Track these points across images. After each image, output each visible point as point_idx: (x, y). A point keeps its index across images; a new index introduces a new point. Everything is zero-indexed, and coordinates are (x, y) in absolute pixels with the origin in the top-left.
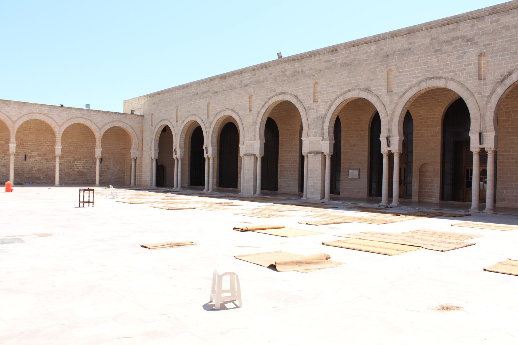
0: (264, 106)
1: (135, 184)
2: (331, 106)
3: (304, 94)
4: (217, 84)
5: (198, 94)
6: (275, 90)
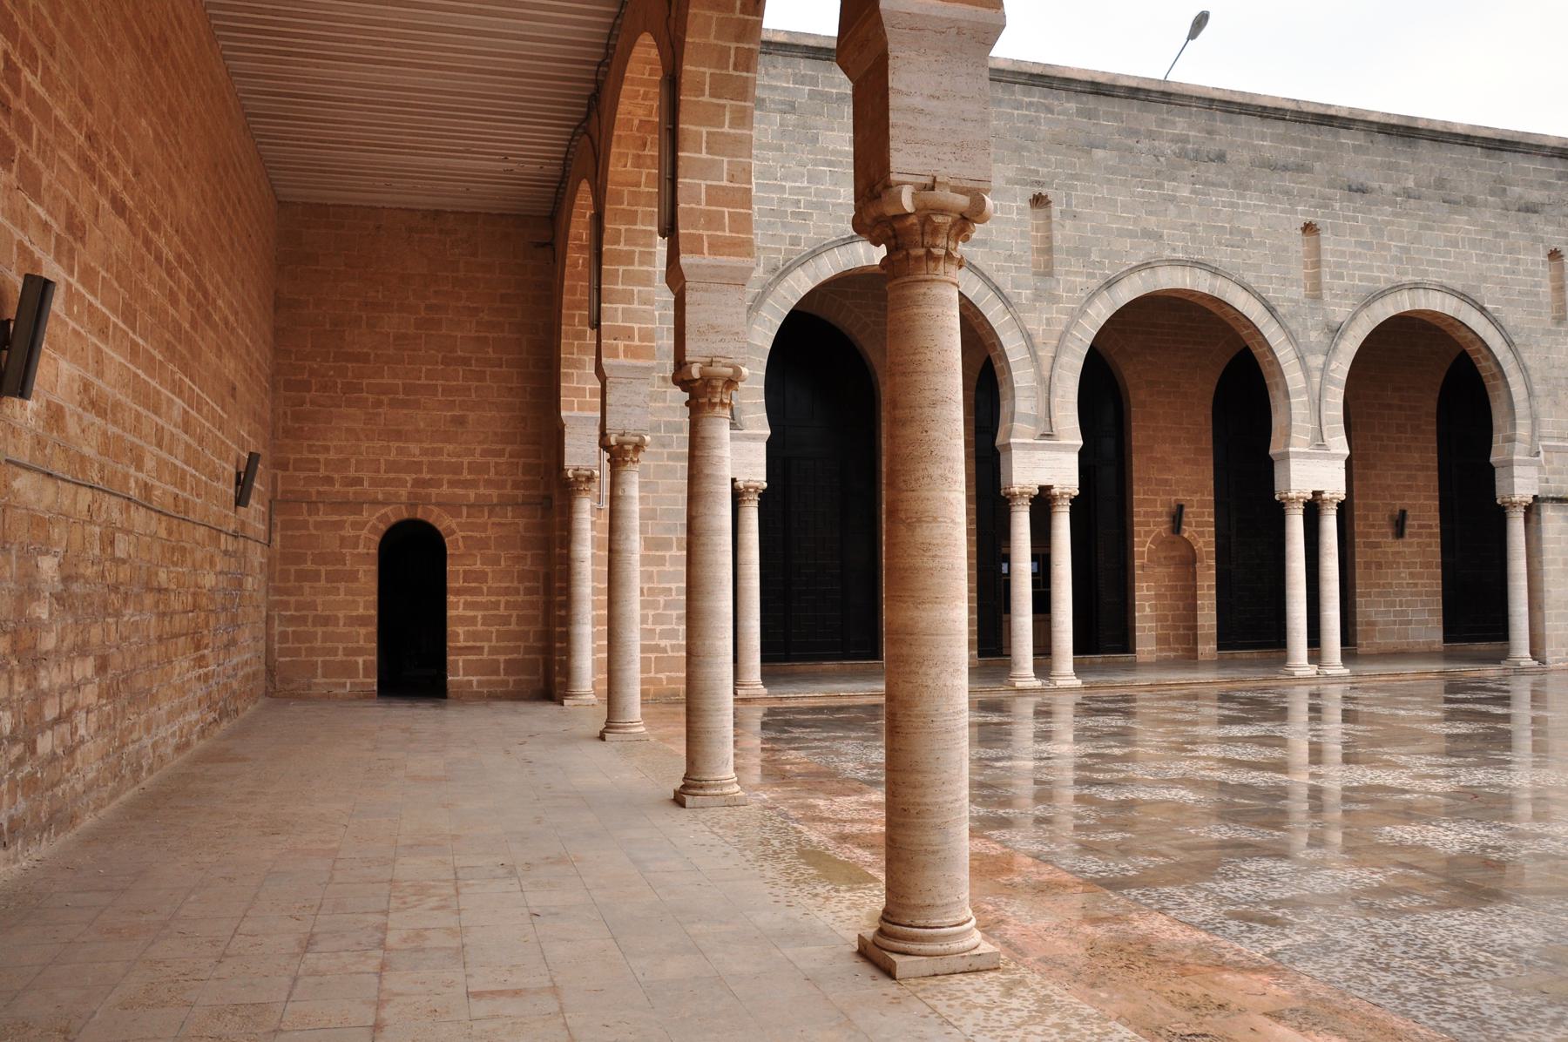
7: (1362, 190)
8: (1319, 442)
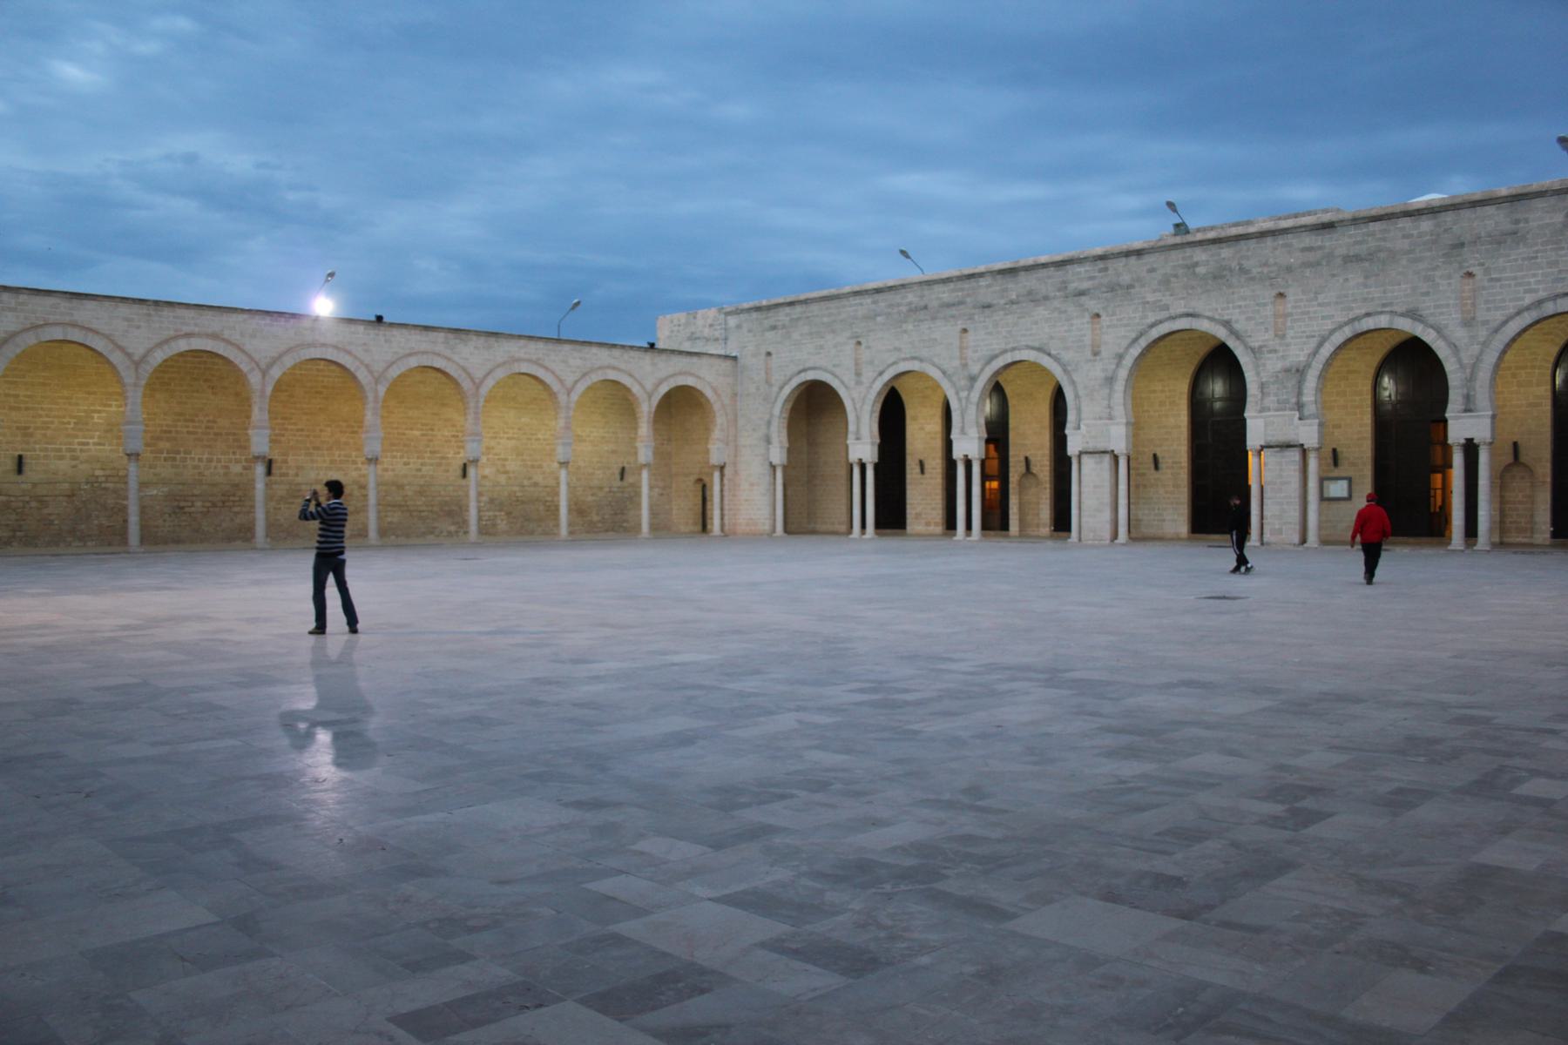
0: (1135, 340)
1: (722, 530)
2: (1320, 345)
3: (1249, 319)
4: (988, 286)
5: (926, 307)
6: (1166, 308)
7: (989, 306)
8: (963, 431)
